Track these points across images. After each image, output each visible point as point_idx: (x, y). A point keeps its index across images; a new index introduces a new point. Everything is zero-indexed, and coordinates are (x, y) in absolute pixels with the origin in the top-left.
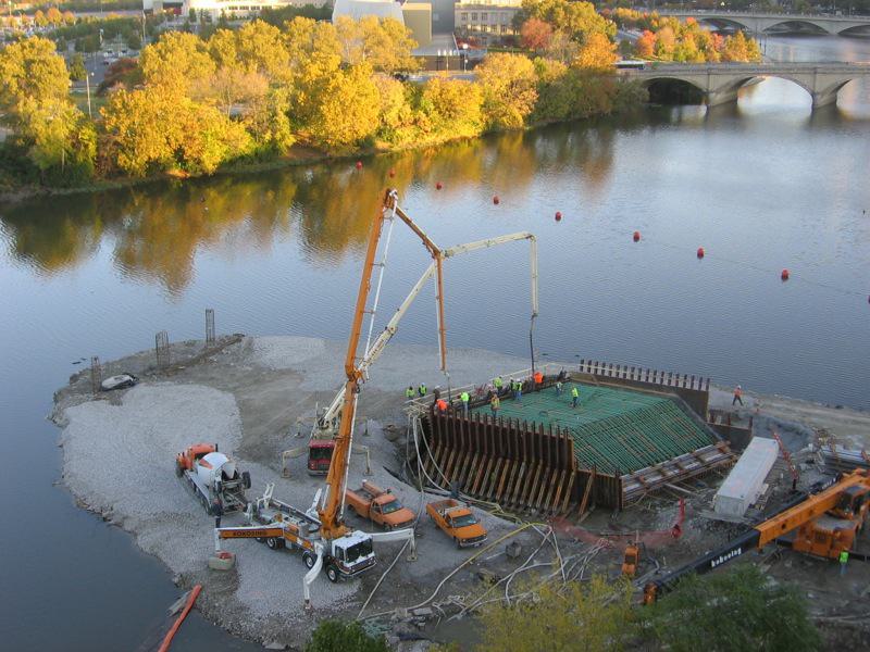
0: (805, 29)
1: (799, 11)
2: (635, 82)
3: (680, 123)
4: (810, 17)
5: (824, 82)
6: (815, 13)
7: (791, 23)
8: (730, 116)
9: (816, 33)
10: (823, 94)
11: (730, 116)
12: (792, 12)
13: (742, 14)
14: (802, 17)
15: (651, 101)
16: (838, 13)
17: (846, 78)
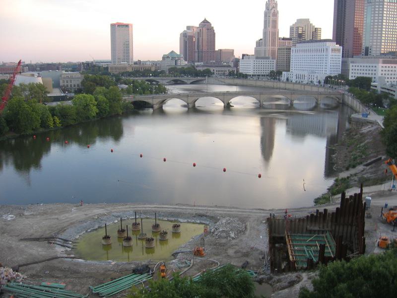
0: (179, 82)
1: (177, 76)
2: (129, 102)
3: (144, 115)
4: (181, 78)
5: (191, 100)
6: (182, 77)
7: (174, 81)
8: (161, 112)
9: (183, 83)
10: (191, 103)
11: (161, 112)
12: (175, 76)
13: (158, 78)
14: (178, 78)
15: (134, 108)
16: (189, 76)
17: (198, 97)
